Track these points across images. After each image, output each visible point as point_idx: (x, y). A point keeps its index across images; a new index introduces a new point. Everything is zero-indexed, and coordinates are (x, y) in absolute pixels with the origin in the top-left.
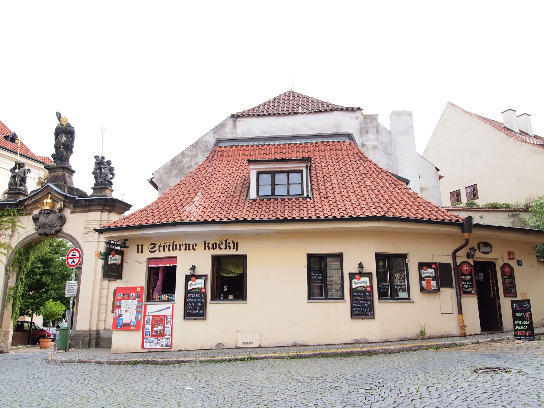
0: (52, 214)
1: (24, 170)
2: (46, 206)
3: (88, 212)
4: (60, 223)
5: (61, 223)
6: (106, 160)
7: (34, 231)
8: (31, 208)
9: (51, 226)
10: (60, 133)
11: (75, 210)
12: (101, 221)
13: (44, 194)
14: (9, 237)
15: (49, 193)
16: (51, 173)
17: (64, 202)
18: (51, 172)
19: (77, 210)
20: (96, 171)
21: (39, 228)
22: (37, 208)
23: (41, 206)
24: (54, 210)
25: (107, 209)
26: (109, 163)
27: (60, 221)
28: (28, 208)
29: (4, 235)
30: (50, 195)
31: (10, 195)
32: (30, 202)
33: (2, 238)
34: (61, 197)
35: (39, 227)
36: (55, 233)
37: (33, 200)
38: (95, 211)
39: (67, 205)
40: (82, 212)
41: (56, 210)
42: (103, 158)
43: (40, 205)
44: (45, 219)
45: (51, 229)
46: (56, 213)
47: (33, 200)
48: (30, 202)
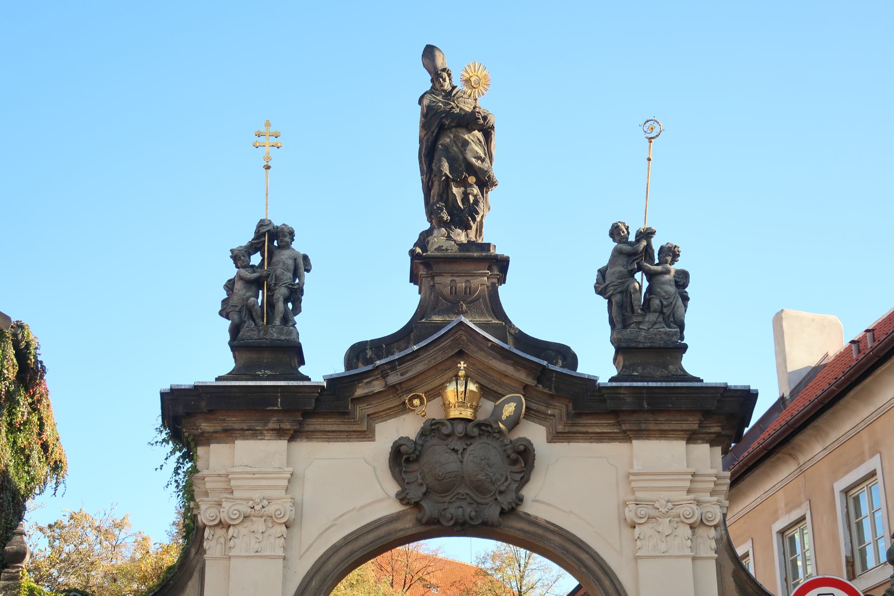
0: (484, 439)
1: (295, 259)
2: (462, 405)
3: (626, 437)
4: (518, 477)
5: (522, 478)
6: (656, 244)
7: (394, 507)
8: (371, 411)
9: (480, 489)
10: (450, 128)
11: (574, 429)
12: (694, 475)
13: (439, 359)
14: (284, 528)
15: (461, 354)
16: (438, 279)
17: (526, 389)
18: (440, 274)
19: (584, 429)
20: (622, 283)
21: (425, 494)
22: (403, 409)
23: (422, 403)
24: (494, 426)
25: (713, 430)
26: (670, 253)
27: (516, 468)
28: (361, 410)
29: (261, 517)
30: (462, 365)
31: (254, 356)
32: (377, 386)
33: (254, 528)
34: (522, 376)
35: (424, 489)
36: (501, 520)
37: (393, 379)
38: (663, 434)
39: (534, 406)
40: (601, 437)
41: (501, 425)
42: (646, 234)
43: (416, 402)
44: (453, 457)
45: (479, 500)
46: (497, 436)
47: (393, 379)
48: (377, 386)
